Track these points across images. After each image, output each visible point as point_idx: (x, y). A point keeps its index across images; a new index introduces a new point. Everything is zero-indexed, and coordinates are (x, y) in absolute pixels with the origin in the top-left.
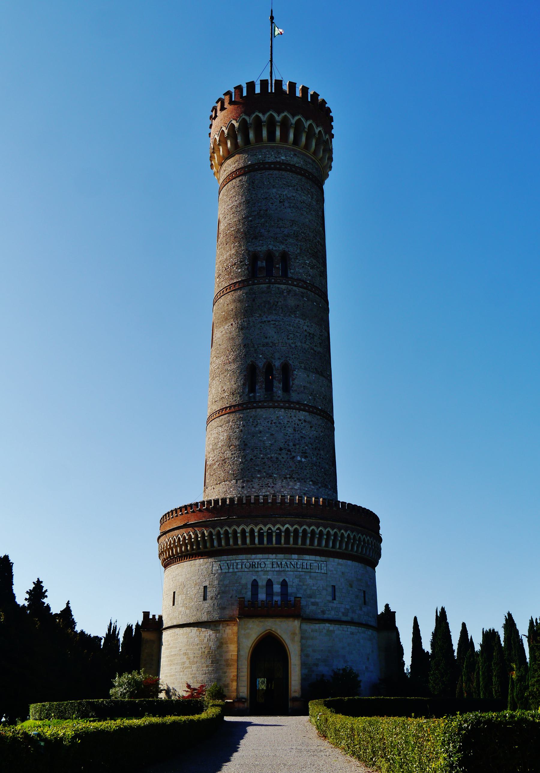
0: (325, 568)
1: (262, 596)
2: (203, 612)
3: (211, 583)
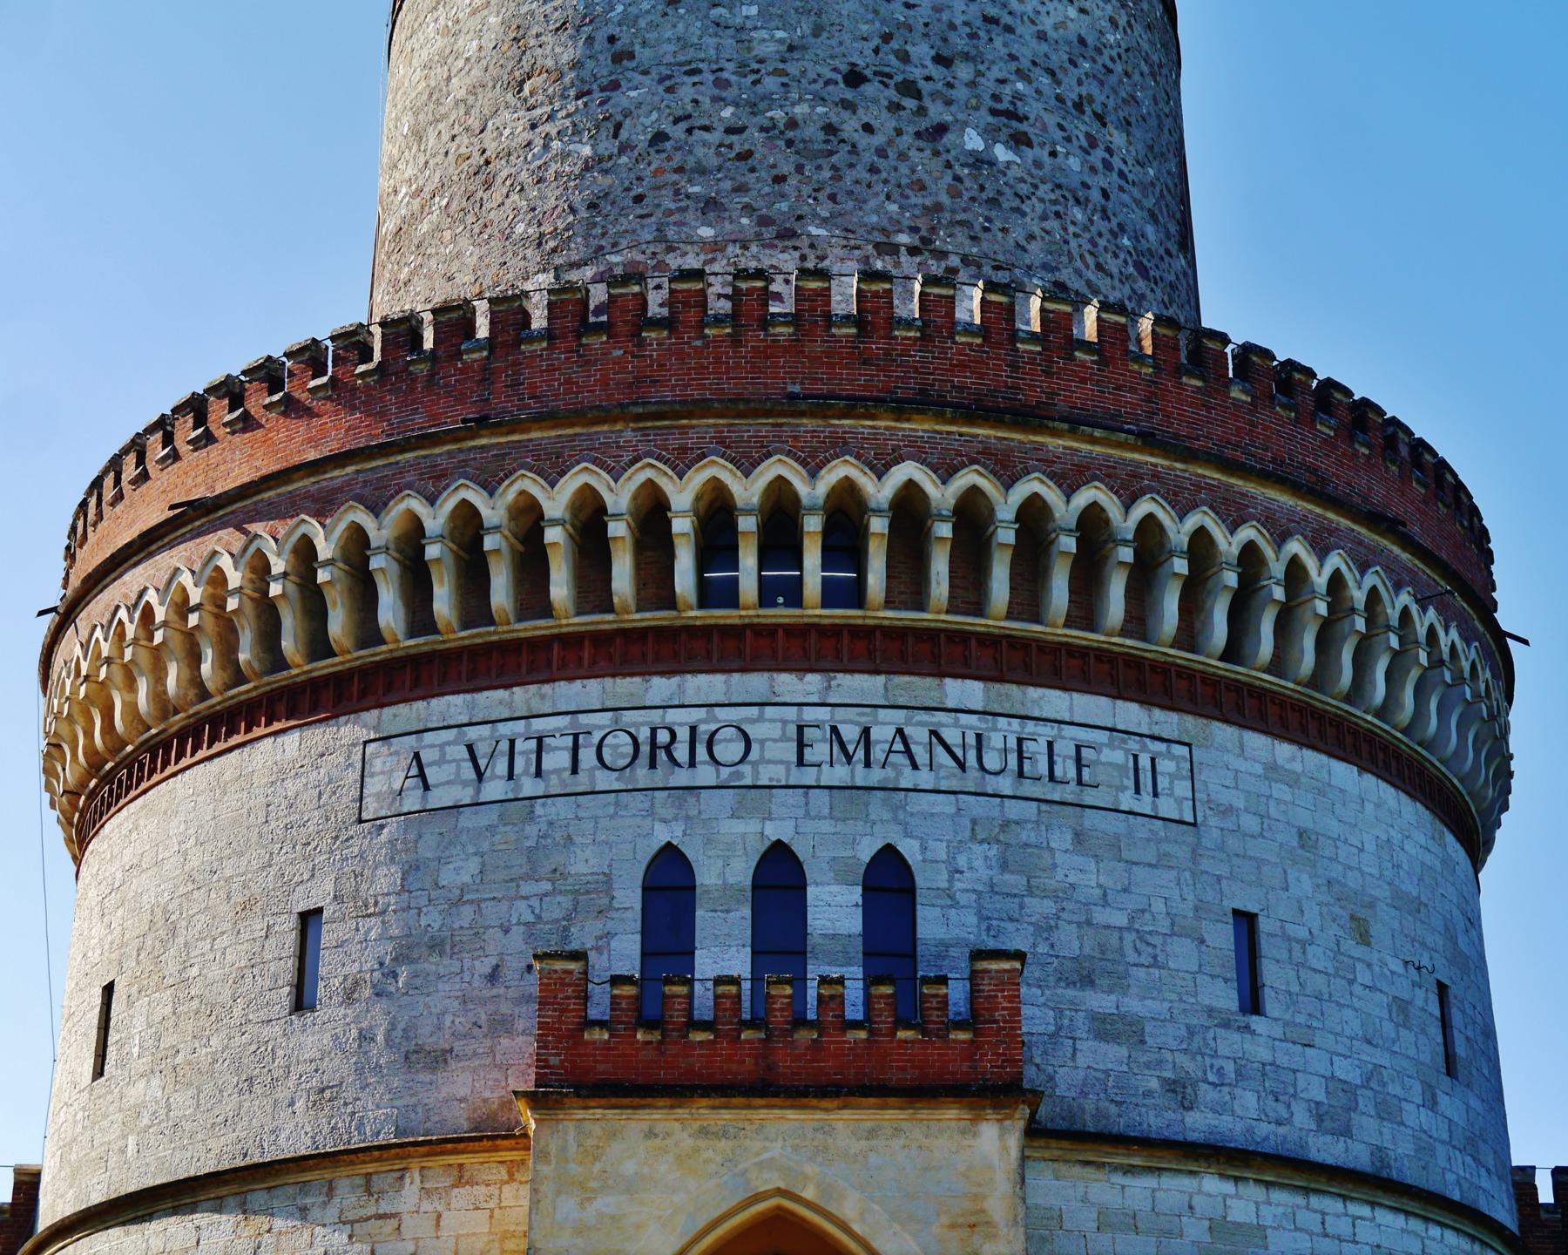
0: (1183, 788)
1: (723, 951)
2: (282, 1094)
3: (348, 886)
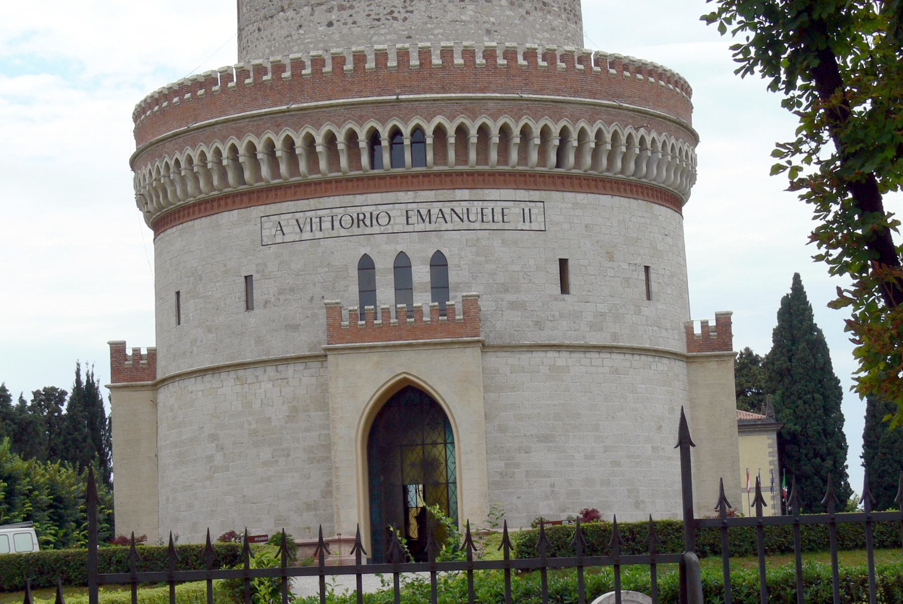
1: (386, 295)
